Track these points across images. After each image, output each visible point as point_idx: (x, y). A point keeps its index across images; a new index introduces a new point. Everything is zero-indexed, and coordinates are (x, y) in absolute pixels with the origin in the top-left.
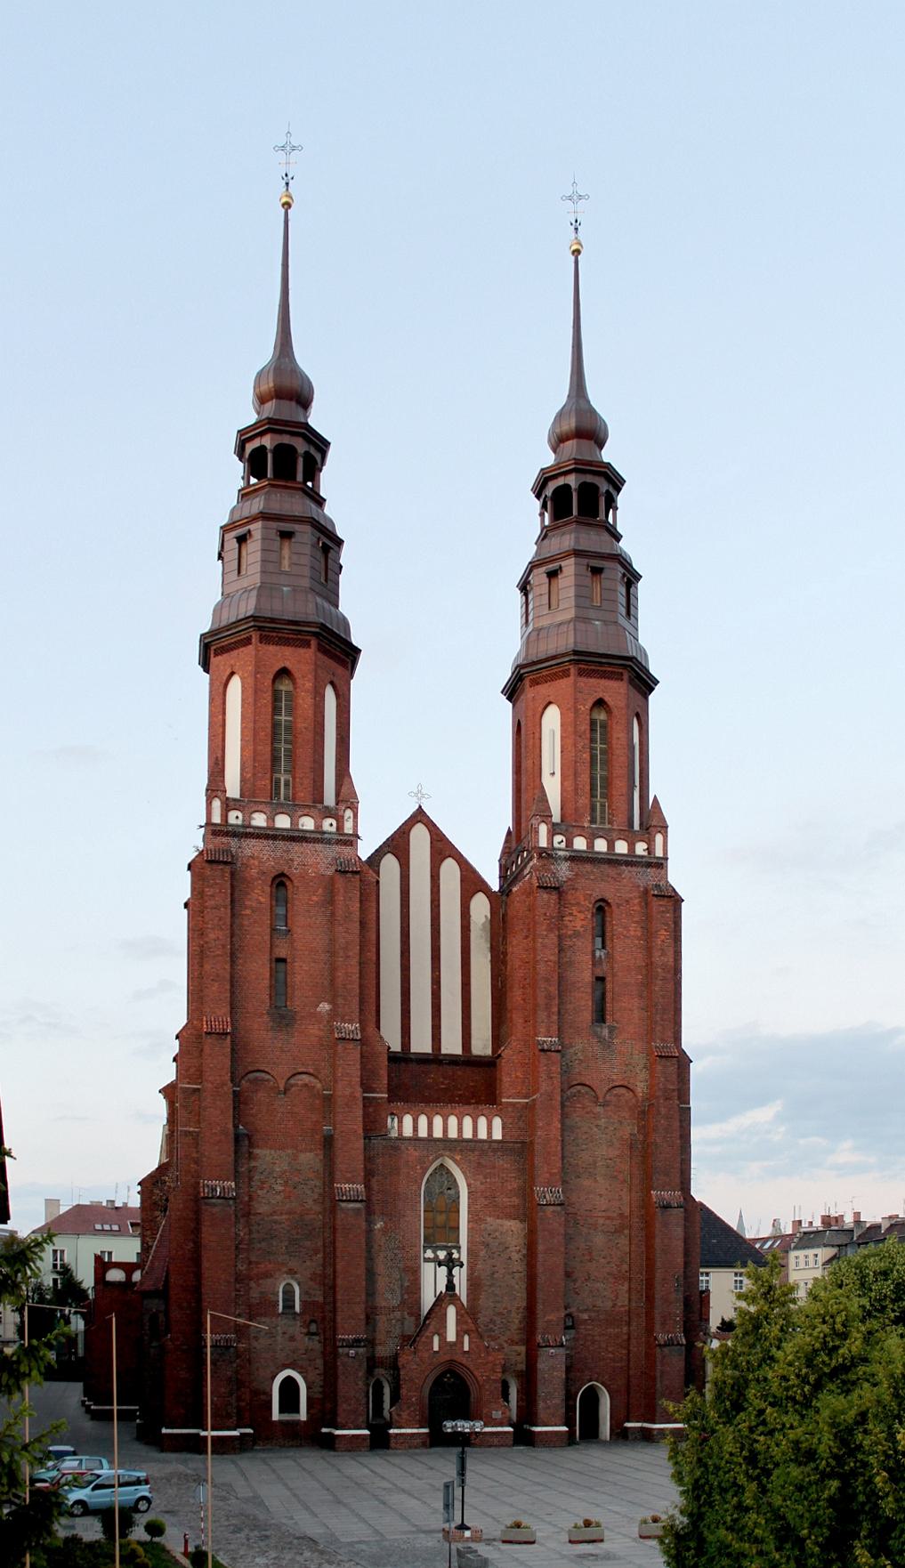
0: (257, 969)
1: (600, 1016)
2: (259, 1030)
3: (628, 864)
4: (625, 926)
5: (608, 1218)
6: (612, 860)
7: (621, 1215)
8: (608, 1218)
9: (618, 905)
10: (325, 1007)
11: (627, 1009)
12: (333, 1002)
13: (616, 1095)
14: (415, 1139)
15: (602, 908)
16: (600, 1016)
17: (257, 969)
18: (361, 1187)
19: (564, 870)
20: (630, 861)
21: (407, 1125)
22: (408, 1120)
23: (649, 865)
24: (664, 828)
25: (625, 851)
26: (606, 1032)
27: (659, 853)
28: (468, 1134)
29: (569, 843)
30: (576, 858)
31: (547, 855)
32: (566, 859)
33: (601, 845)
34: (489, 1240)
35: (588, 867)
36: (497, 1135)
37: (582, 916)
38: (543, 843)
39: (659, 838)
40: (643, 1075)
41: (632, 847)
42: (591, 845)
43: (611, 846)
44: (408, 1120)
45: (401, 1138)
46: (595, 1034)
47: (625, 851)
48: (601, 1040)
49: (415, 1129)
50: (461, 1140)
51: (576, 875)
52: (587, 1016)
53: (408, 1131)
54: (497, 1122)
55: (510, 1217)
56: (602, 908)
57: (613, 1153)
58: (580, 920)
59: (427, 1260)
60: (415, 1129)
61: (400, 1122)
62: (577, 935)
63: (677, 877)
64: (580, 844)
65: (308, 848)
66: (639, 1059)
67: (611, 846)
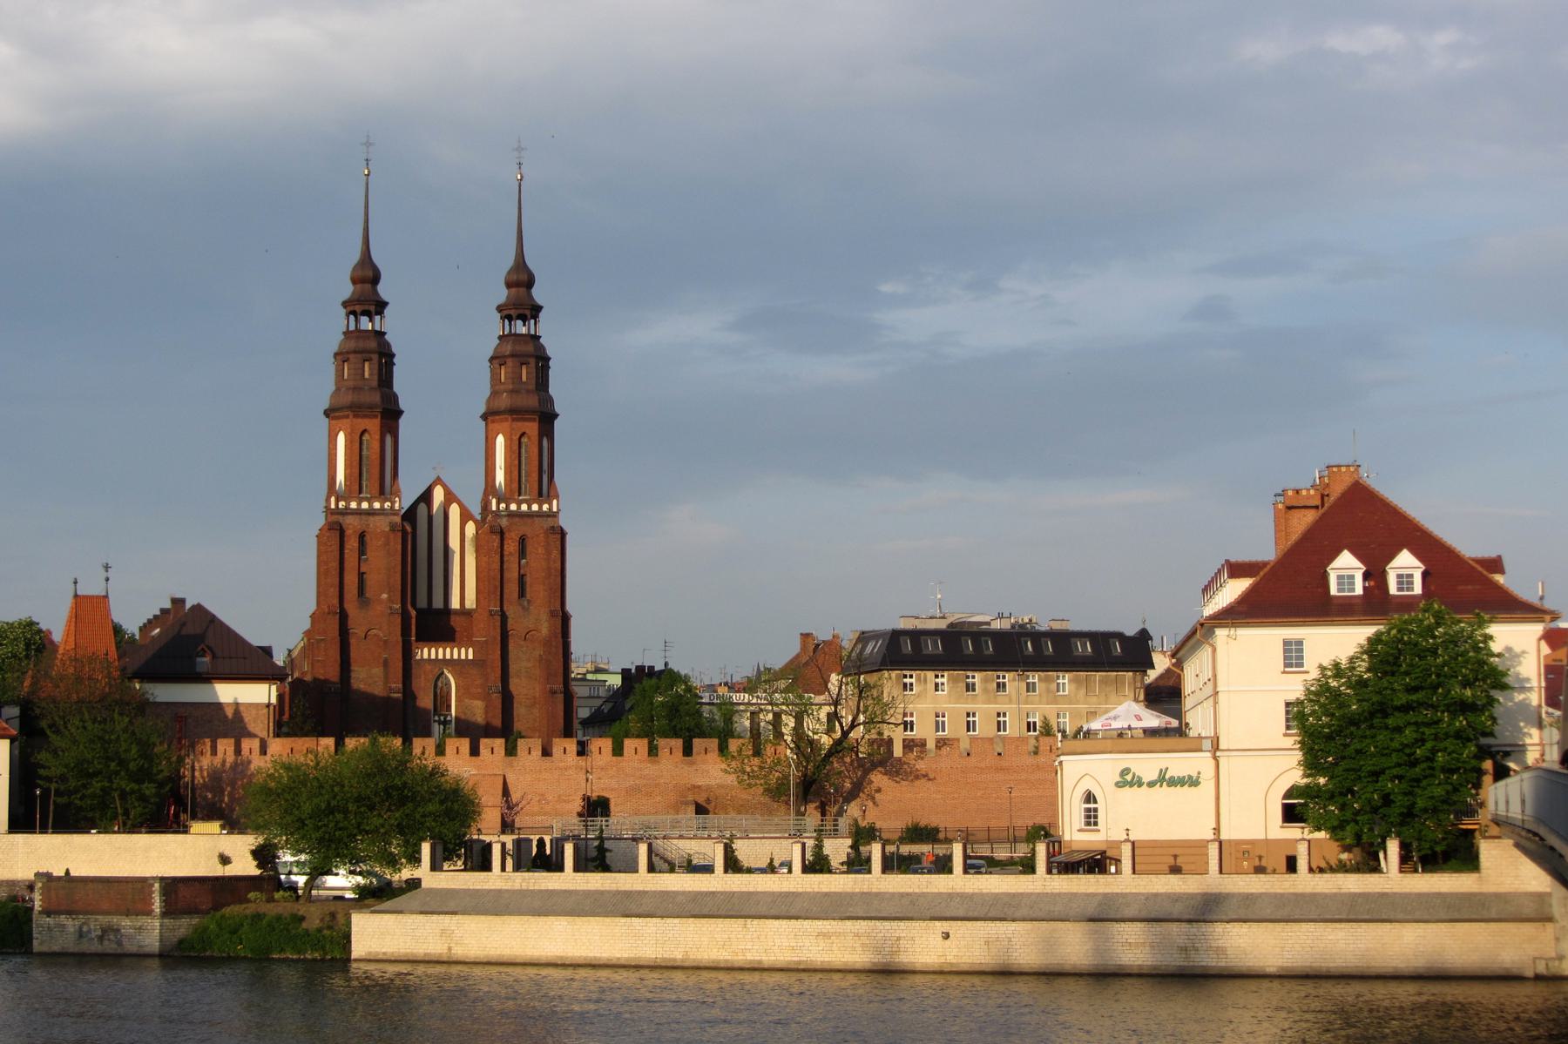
0: (351, 579)
1: (522, 594)
2: (351, 607)
3: (537, 516)
4: (536, 550)
5: (527, 699)
6: (530, 515)
7: (534, 697)
8: (527, 699)
9: (533, 538)
10: (385, 596)
11: (538, 591)
12: (388, 593)
13: (532, 635)
14: (429, 660)
15: (522, 541)
16: (522, 594)
17: (351, 579)
18: (401, 686)
19: (504, 522)
20: (540, 514)
21: (426, 653)
22: (426, 650)
23: (549, 516)
24: (557, 497)
25: (537, 509)
26: (526, 603)
27: (555, 509)
28: (456, 657)
29: (508, 507)
30: (511, 515)
31: (497, 514)
32: (505, 516)
33: (524, 507)
34: (466, 711)
35: (517, 519)
36: (471, 657)
37: (513, 544)
38: (494, 508)
39: (555, 502)
40: (546, 624)
41: (540, 507)
42: (519, 507)
43: (529, 507)
44: (426, 650)
45: (422, 659)
46: (520, 605)
47: (537, 509)
48: (523, 608)
49: (429, 654)
50: (452, 660)
51: (511, 524)
52: (516, 595)
53: (426, 656)
54: (471, 650)
55: (478, 699)
56: (522, 541)
57: (530, 665)
58: (511, 547)
59: (435, 721)
60: (429, 654)
61: (422, 651)
62: (511, 554)
63: (563, 522)
64: (513, 507)
65: (377, 518)
66: (544, 617)
67: (529, 507)
